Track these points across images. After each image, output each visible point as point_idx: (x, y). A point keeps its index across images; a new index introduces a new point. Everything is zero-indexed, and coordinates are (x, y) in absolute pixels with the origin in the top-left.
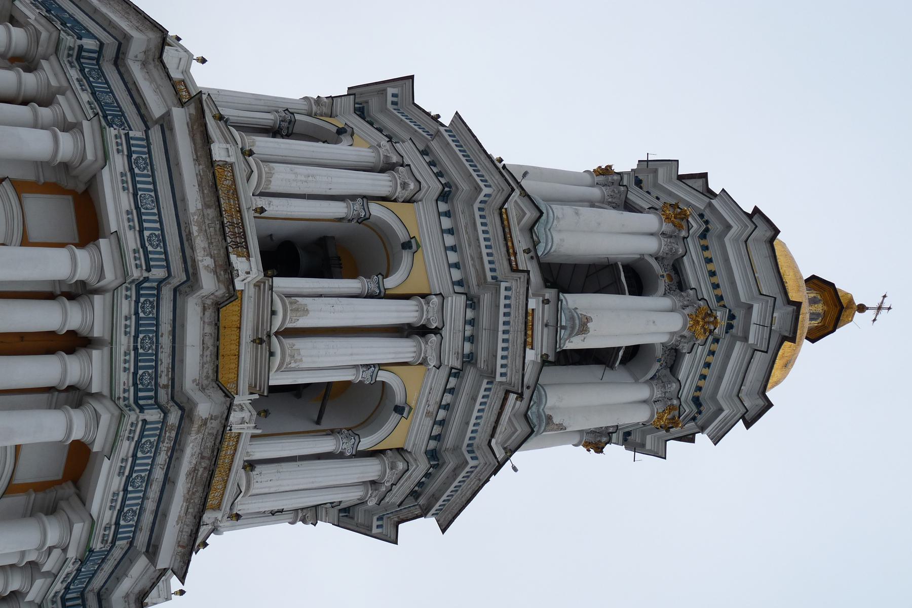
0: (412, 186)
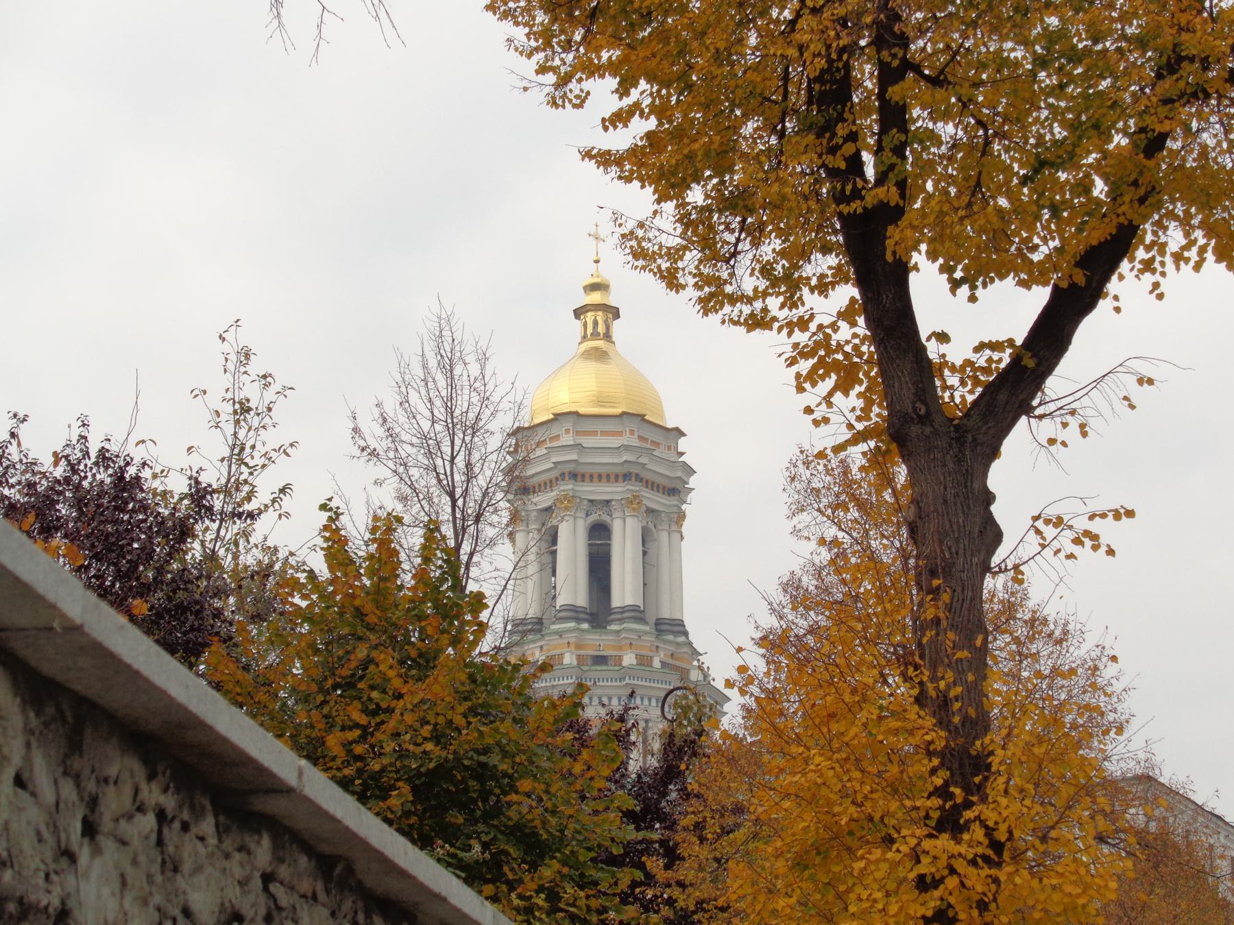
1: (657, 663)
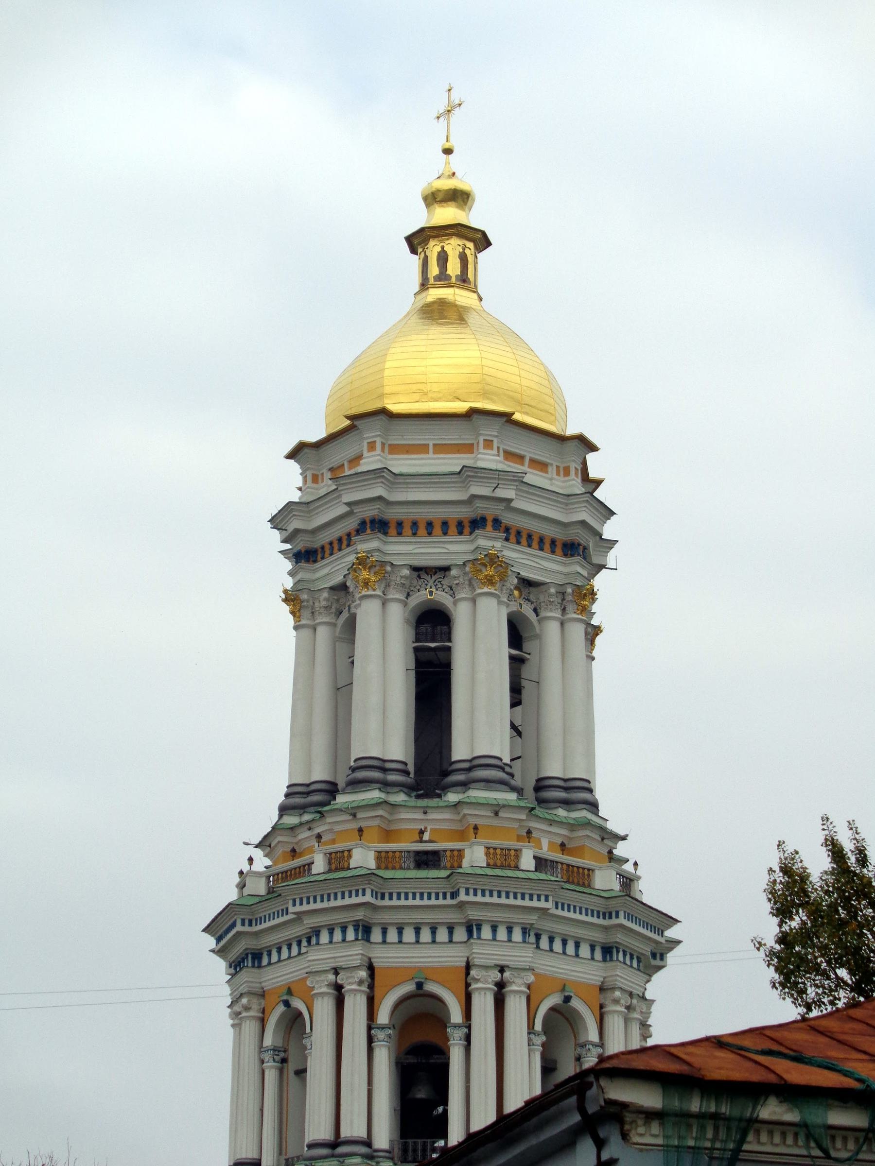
0: (244, 1001)
1: (527, 862)
